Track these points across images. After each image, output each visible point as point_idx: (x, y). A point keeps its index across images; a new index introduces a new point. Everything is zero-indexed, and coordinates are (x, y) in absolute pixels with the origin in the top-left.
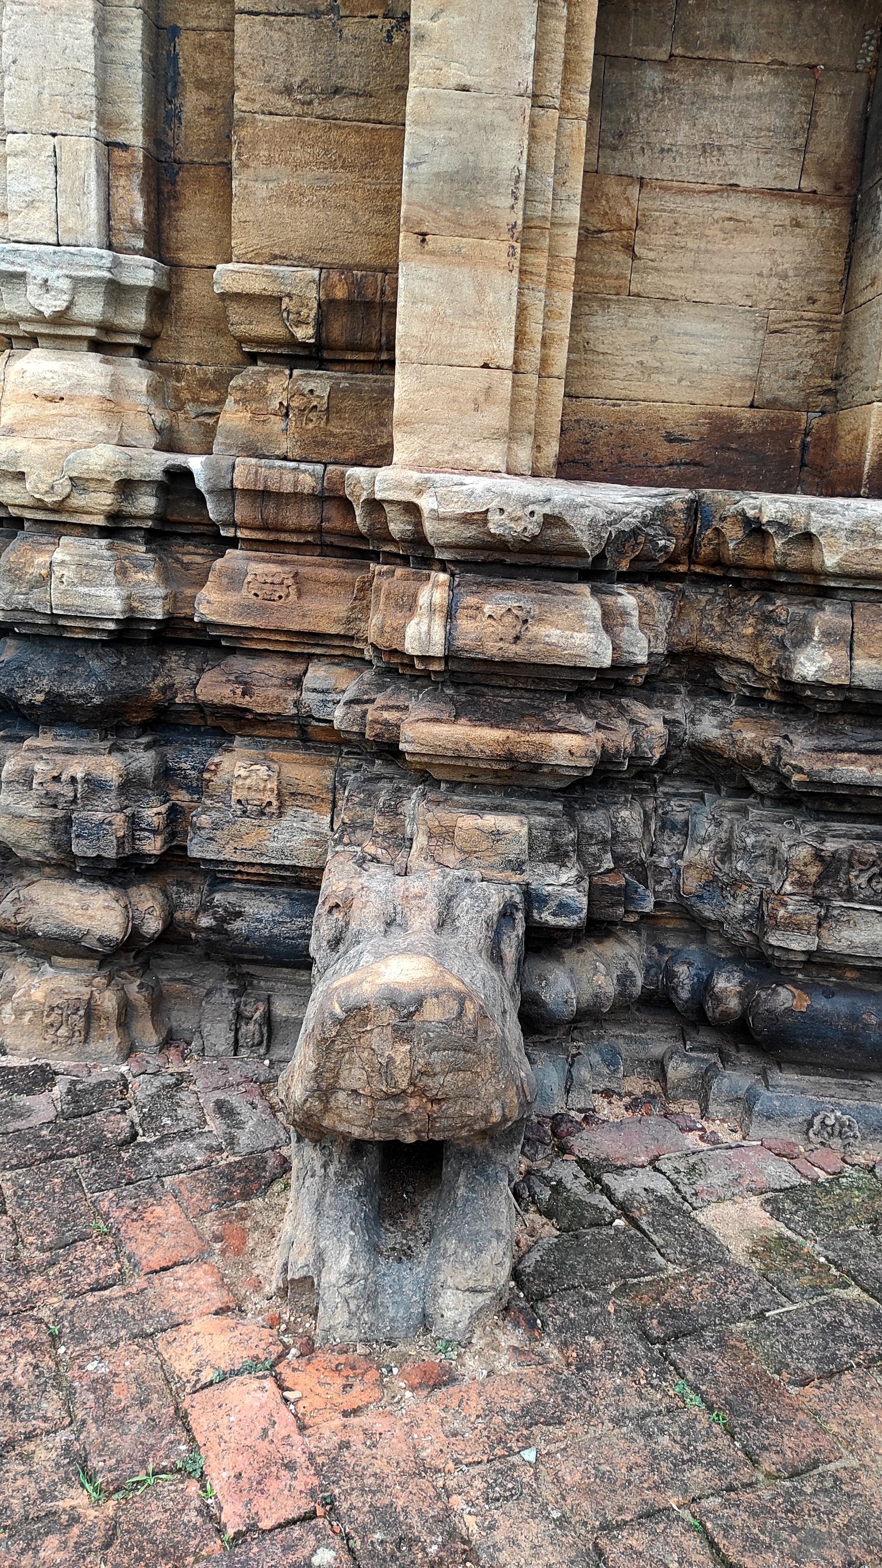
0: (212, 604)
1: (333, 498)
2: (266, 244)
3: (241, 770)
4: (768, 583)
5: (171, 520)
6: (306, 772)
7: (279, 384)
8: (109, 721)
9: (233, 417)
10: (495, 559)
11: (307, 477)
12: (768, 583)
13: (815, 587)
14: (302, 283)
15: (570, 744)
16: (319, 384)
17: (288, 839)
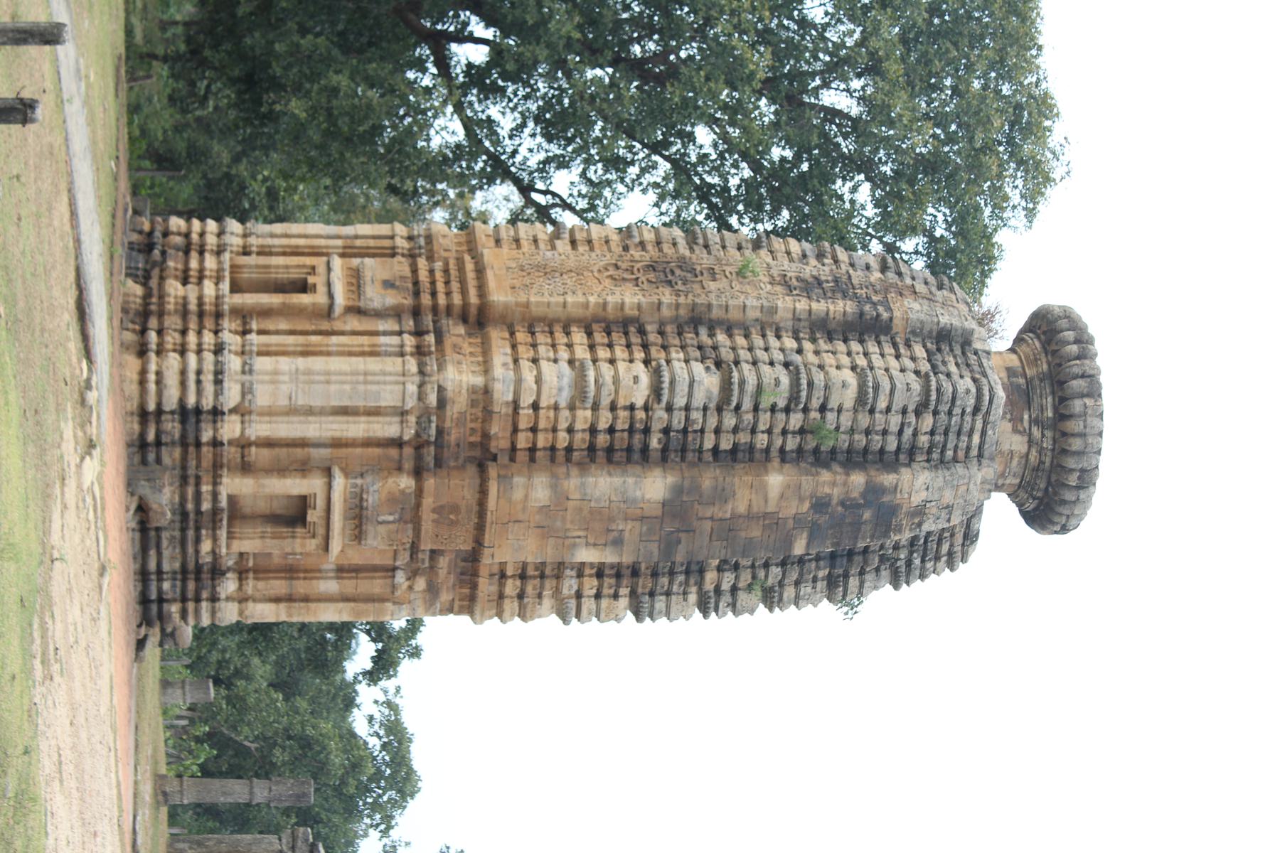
0: (204, 449)
1: (221, 467)
2: (258, 455)
3: (177, 452)
4: (214, 522)
5: (216, 443)
6: (178, 462)
7: (239, 455)
8: (183, 436)
9: (233, 449)
10: (215, 495)
11: (225, 461)
12: (214, 522)
13: (214, 529)
14: (253, 458)
15: (190, 506)
16: (239, 460)
17: (166, 460)
